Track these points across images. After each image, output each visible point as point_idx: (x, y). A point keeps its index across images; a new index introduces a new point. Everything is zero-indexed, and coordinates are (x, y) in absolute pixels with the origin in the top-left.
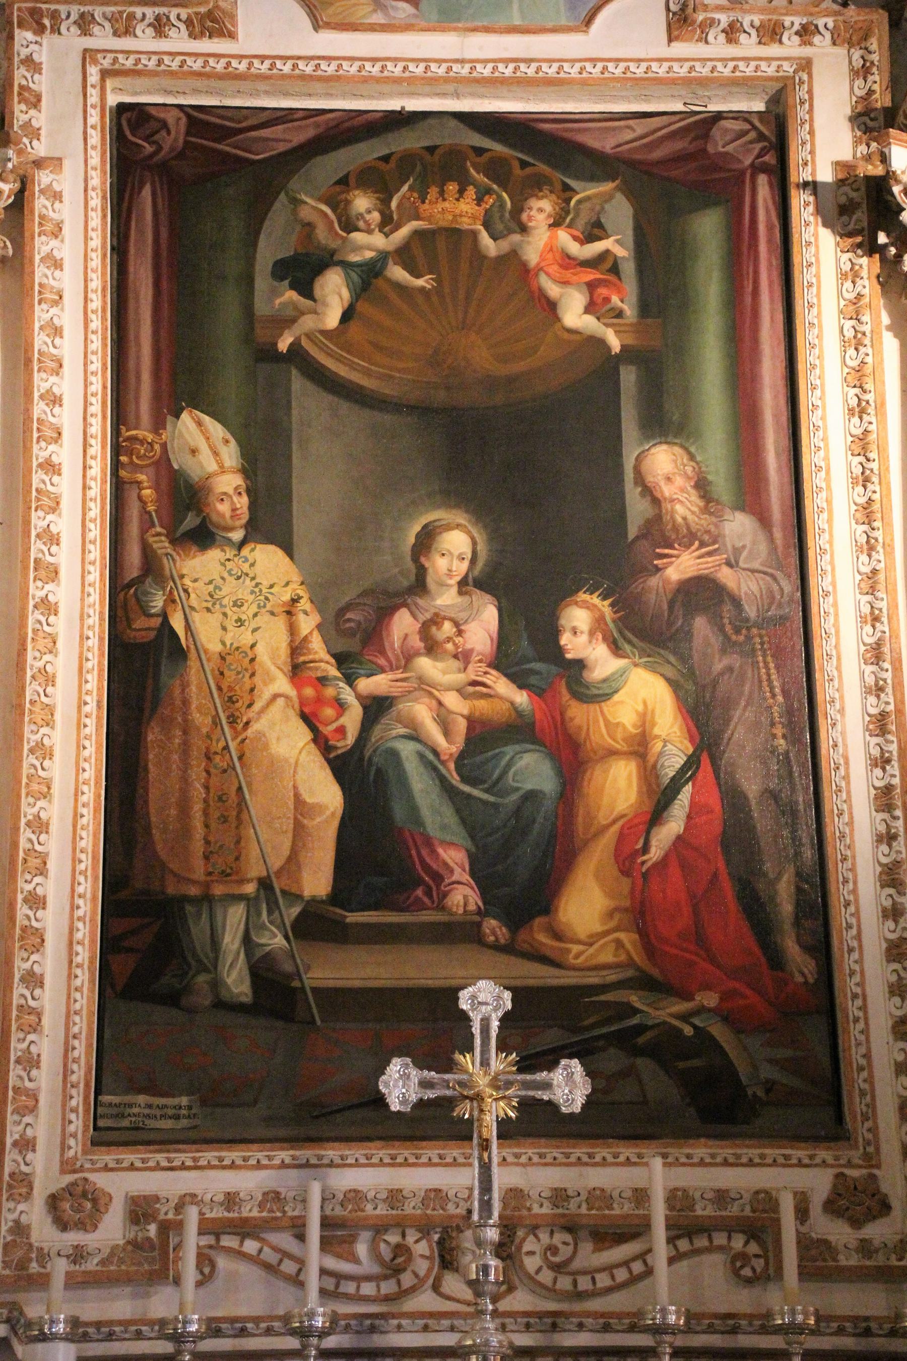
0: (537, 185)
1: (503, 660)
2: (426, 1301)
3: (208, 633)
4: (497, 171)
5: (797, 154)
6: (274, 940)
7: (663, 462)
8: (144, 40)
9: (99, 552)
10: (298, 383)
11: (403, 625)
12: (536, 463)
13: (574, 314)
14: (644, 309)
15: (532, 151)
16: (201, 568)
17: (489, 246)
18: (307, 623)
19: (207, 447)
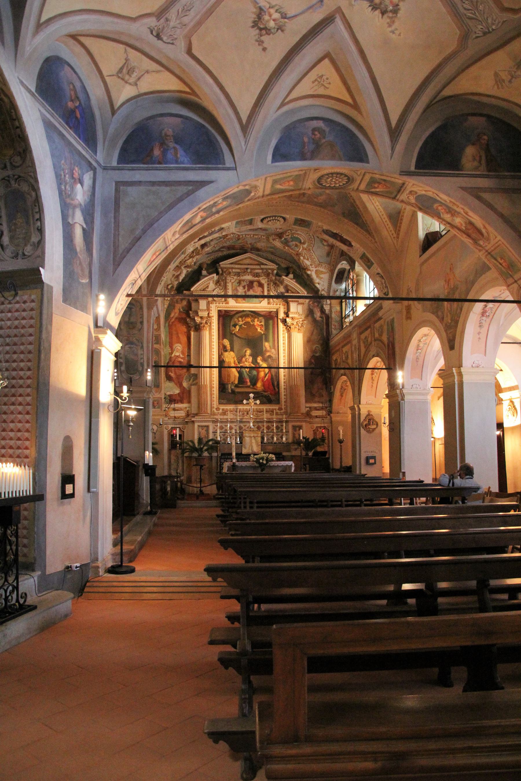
0: (256, 317)
1: (252, 362)
2: (246, 417)
3: (227, 360)
4: (252, 316)
5: (279, 316)
6: (233, 387)
7: (267, 344)
8: (221, 305)
9: (217, 353)
10: (234, 336)
11: (244, 359)
12: (255, 344)
13: (259, 330)
14: (265, 330)
15: (255, 314)
16: (226, 354)
17: (251, 323)
18: (235, 359)
19: (226, 342)
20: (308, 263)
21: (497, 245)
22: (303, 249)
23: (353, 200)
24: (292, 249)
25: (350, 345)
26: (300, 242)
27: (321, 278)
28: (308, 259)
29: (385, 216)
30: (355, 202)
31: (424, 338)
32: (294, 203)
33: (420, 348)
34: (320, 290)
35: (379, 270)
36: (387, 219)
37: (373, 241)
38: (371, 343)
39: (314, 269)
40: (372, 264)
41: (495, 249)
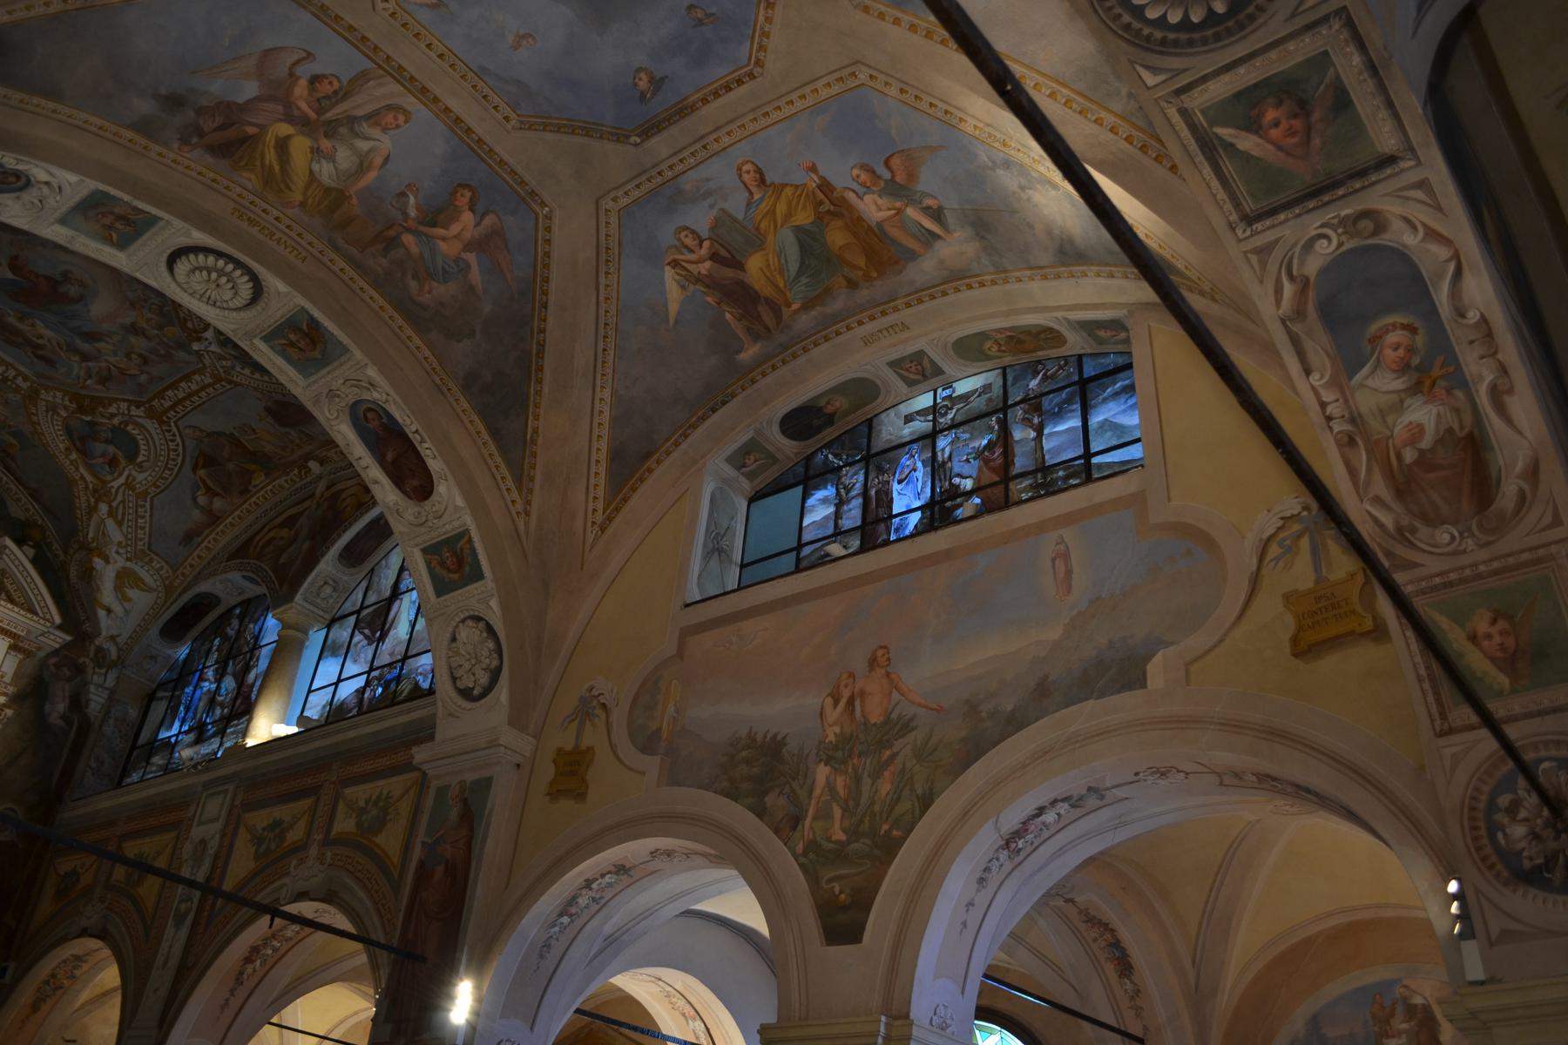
20: (115, 533)
21: (1541, 552)
22: (128, 485)
24: (89, 467)
25: (172, 835)
26: (132, 456)
27: (125, 599)
28: (120, 524)
29: (604, 445)
31: (607, 879)
32: (333, 255)
33: (573, 910)
34: (104, 633)
35: (494, 603)
36: (603, 456)
37: (519, 506)
38: (300, 848)
39: (120, 562)
40: (478, 575)
41: (1496, 572)
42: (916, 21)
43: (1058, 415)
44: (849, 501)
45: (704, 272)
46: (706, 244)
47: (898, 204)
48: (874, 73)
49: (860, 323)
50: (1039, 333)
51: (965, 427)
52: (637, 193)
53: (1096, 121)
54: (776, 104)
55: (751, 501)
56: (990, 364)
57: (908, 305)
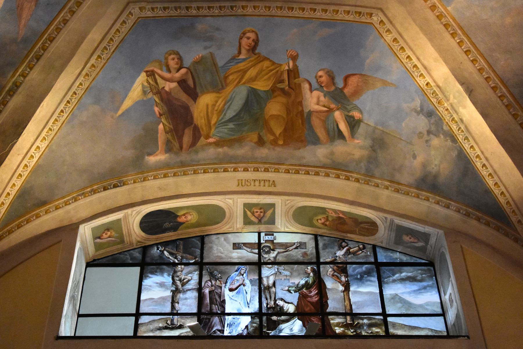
23: (16, 86)
29: (19, 183)
30: (12, 92)
42: (438, 4)
43: (361, 279)
44: (184, 292)
45: (167, 89)
46: (183, 71)
47: (333, 106)
48: (385, 20)
49: (246, 170)
50: (361, 223)
51: (286, 267)
52: (161, 13)
53: (513, 115)
54: (303, 6)
55: (89, 264)
56: (308, 230)
57: (287, 171)
